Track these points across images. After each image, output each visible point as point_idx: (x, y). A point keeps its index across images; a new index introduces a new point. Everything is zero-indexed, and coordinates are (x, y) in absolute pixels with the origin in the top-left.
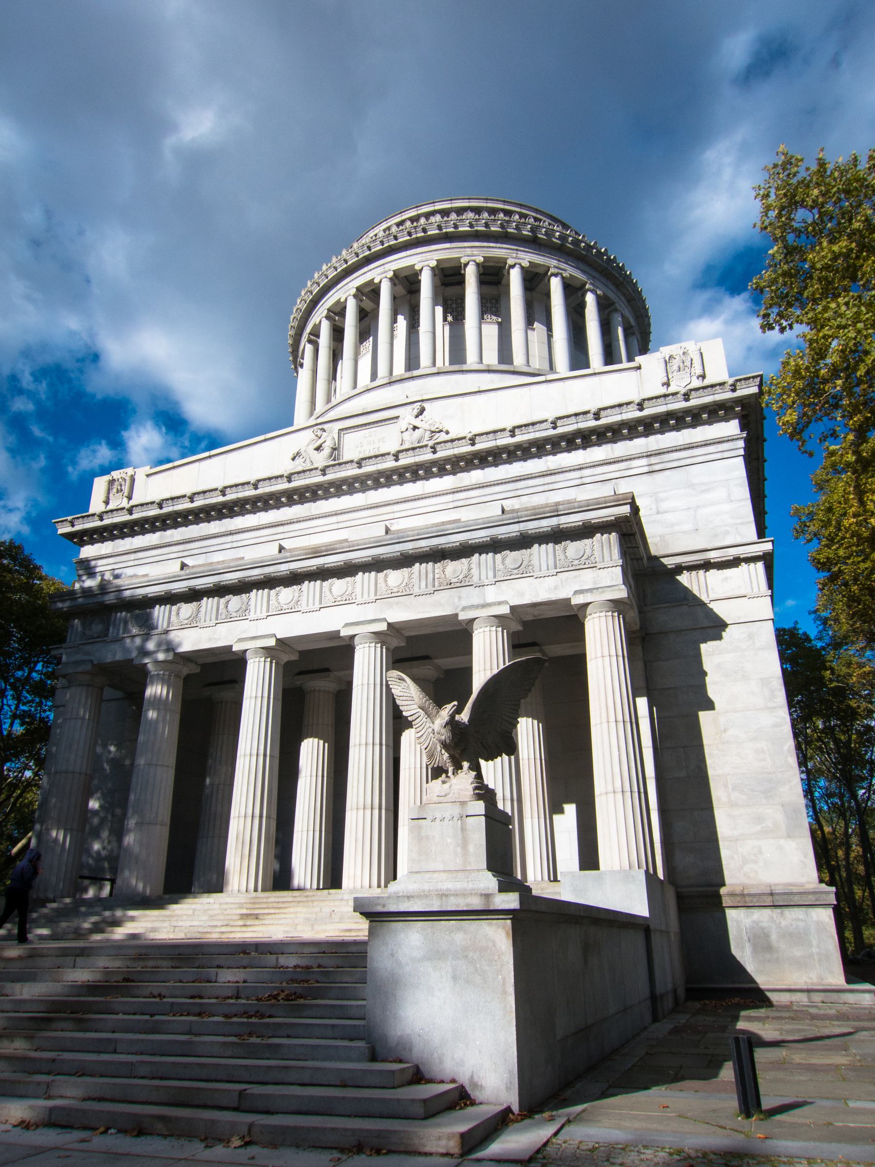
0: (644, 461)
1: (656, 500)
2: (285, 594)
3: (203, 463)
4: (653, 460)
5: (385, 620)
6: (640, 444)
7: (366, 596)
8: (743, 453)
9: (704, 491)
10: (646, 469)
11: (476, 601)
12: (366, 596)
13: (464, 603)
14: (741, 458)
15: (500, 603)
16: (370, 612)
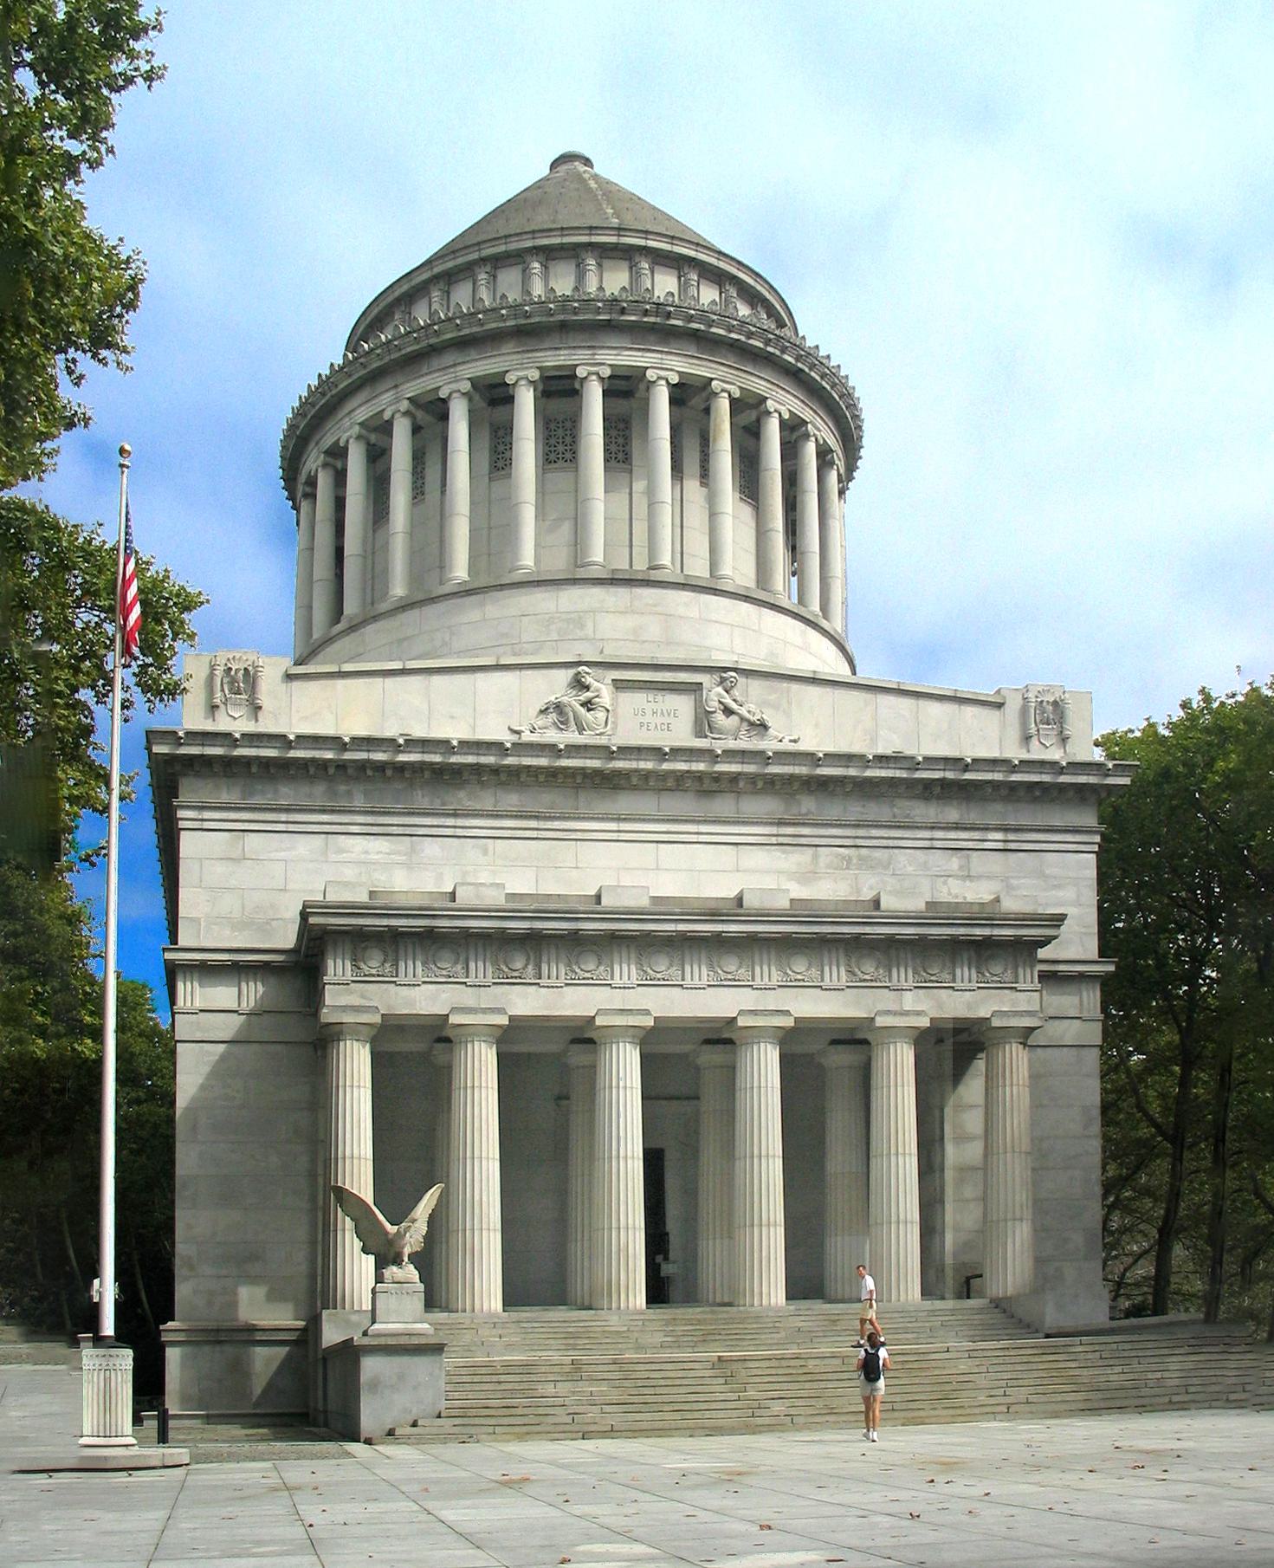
0: (999, 836)
1: (1007, 886)
2: (662, 965)
3: (390, 682)
4: (1011, 837)
5: (787, 1013)
6: (996, 812)
7: (766, 979)
8: (1097, 850)
9: (1055, 887)
10: (1000, 846)
11: (894, 1007)
12: (766, 979)
13: (880, 1007)
14: (1094, 856)
15: (918, 1013)
16: (771, 1001)
